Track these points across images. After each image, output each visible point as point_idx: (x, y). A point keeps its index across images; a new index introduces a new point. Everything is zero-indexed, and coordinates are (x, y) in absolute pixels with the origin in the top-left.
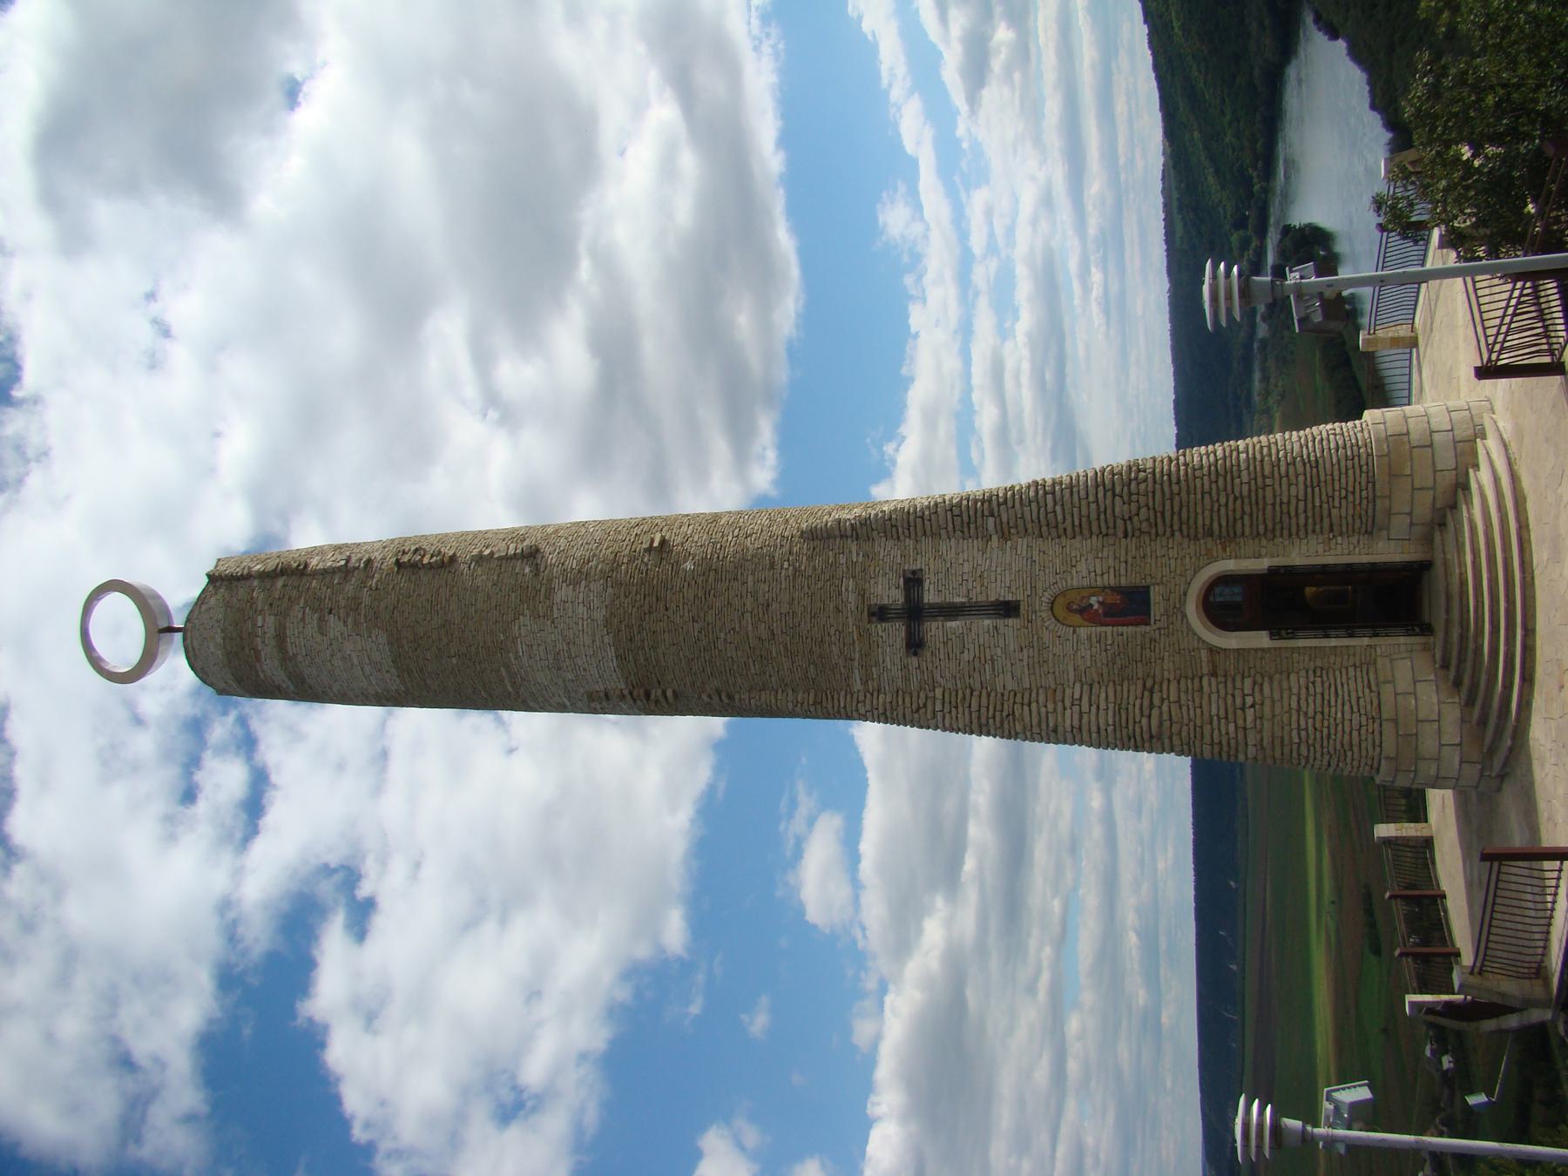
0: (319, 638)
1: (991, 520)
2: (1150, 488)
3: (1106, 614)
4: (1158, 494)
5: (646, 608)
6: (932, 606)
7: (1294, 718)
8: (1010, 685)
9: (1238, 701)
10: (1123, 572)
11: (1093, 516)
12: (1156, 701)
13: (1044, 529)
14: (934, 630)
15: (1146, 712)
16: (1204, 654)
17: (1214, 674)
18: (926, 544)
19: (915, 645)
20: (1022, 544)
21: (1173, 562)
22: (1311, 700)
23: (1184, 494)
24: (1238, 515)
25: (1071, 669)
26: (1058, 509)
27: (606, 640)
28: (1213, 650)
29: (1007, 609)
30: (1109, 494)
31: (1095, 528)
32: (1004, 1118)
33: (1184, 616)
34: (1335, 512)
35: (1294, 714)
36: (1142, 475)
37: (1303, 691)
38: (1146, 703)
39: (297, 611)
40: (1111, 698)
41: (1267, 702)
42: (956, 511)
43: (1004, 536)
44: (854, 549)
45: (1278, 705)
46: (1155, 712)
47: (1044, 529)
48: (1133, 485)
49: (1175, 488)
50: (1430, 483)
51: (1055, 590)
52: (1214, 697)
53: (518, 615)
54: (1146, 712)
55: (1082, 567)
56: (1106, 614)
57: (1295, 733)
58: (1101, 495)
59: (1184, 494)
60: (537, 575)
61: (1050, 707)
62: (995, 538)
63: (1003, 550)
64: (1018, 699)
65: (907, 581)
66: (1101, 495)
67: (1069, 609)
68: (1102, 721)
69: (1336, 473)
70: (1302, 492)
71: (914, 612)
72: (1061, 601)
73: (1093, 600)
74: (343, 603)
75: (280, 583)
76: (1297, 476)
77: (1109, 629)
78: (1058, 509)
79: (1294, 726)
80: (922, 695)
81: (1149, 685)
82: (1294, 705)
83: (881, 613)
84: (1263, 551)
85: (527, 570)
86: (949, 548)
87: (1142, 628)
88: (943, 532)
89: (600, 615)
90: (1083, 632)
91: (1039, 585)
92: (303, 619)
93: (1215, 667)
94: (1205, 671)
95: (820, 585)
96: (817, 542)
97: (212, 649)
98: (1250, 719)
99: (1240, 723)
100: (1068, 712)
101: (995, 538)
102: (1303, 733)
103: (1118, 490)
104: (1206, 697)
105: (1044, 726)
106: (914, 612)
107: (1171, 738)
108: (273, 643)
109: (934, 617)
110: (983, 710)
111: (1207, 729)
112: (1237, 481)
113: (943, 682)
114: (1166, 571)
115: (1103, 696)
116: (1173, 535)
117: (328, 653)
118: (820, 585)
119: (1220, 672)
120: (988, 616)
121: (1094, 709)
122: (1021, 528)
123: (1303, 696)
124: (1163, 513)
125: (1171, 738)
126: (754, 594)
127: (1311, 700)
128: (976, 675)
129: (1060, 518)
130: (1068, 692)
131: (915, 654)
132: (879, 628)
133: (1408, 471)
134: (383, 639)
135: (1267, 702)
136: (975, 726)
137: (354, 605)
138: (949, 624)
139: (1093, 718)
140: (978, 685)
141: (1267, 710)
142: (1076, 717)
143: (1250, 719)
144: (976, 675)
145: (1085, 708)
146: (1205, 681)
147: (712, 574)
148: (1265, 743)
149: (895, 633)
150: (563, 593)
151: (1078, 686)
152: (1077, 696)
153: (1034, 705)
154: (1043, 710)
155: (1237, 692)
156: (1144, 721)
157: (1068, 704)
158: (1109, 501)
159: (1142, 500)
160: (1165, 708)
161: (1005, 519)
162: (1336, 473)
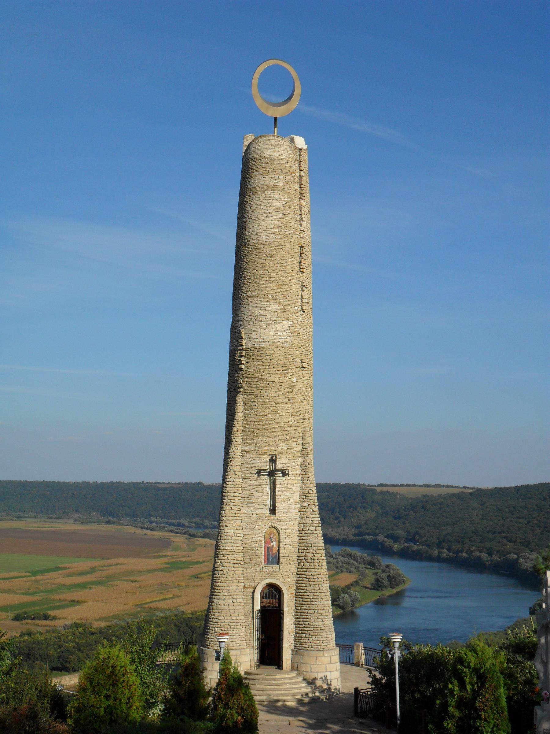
0: (273, 208)
1: (306, 505)
2: (316, 567)
3: (268, 547)
4: (313, 570)
5: (279, 362)
6: (275, 479)
7: (229, 618)
8: (243, 509)
9: (234, 597)
11: (306, 545)
12: (236, 565)
14: (266, 480)
15: (232, 562)
16: (252, 584)
17: (244, 588)
18: (299, 479)
20: (297, 517)
21: (288, 574)
22: (235, 624)
23: (313, 580)
24: (304, 599)
25: (249, 533)
26: (310, 532)
27: (267, 343)
29: (273, 510)
30: (314, 552)
31: (301, 545)
32: (110, 623)
33: (267, 578)
34: (304, 635)
35: (230, 618)
36: (320, 564)
37: (238, 621)
38: (235, 562)
39: (285, 197)
40: (237, 548)
41: (234, 608)
43: (301, 510)
44: (298, 449)
46: (231, 565)
48: (318, 561)
49: (315, 577)
50: (313, 671)
51: (279, 528)
52: (236, 587)
53: (279, 304)
54: (232, 562)
56: (268, 547)
57: (223, 618)
58: (314, 548)
59: (313, 580)
60: (294, 313)
62: (300, 506)
64: (238, 512)
66: (314, 548)
67: (271, 534)
68: (228, 544)
69: (318, 637)
70: (312, 624)
72: (275, 531)
73: (274, 543)
74: (287, 220)
75: (297, 187)
76: (318, 622)
77: (263, 549)
79: (225, 618)
80: (240, 474)
81: (242, 563)
82: (233, 618)
83: (273, 460)
84: (290, 608)
85: (296, 308)
86: (297, 488)
87: (263, 561)
89: (277, 341)
90: (263, 539)
91: (281, 523)
92: (281, 200)
93: (247, 588)
94: (246, 584)
95: (285, 435)
96: (301, 434)
97: (269, 151)
98: (228, 601)
99: (227, 597)
100: (232, 531)
101: (300, 506)
102: (223, 621)
103: (316, 555)
104: (237, 584)
105: (227, 521)
108: (271, 183)
110: (233, 498)
111: (225, 585)
112: (317, 600)
113: (245, 482)
114: (284, 571)
115: (238, 545)
116: (297, 574)
117: (266, 211)
118: (285, 435)
119: (245, 590)
121: (233, 541)
122: (303, 516)
123: (236, 621)
124: (306, 571)
126: (282, 408)
127: (235, 624)
129: (306, 532)
130: (240, 532)
133: (318, 663)
134: (271, 239)
135: (234, 608)
137: (286, 227)
138: (268, 487)
139: (229, 541)
140: (243, 496)
141: (231, 607)
143: (228, 601)
144: (247, 496)
145: (233, 538)
146: (243, 584)
147: (291, 390)
148: (219, 606)
149: (266, 465)
150: (287, 325)
153: (235, 518)
156: (228, 561)
157: (236, 531)
158: (311, 551)
159: (312, 564)
160: (233, 569)
161: (307, 510)
162: (318, 637)
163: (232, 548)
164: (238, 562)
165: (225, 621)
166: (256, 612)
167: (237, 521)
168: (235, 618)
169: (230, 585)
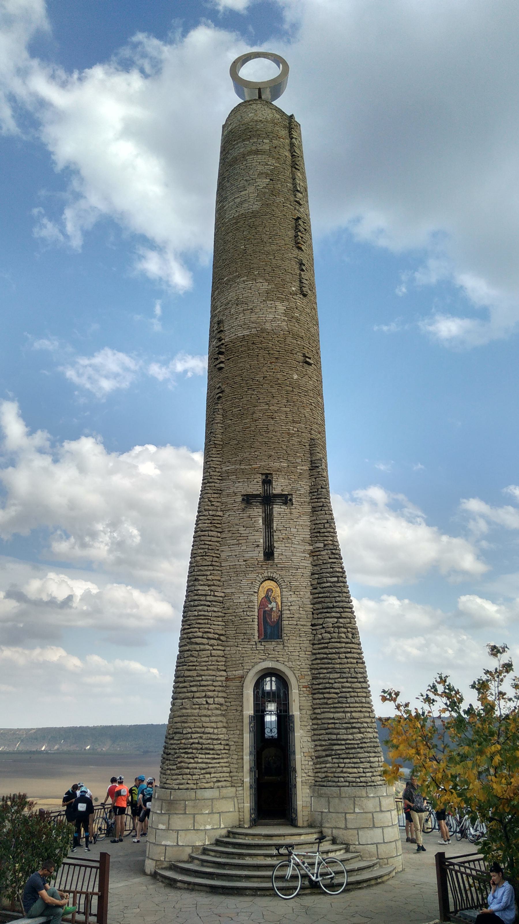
6: (271, 510)
10: (290, 623)
13: (317, 576)
14: (257, 512)
18: (308, 509)
19: (248, 500)
25: (233, 590)
28: (242, 678)
38: (211, 636)
41: (209, 713)
42: (326, 525)
45: (207, 719)
46: (205, 641)
47: (317, 576)
54: (205, 635)
55: (294, 598)
57: (190, 730)
61: (209, 577)
62: (311, 548)
63: (304, 552)
64: (215, 559)
65: (286, 496)
68: (200, 608)
71: (268, 500)
78: (329, 584)
81: (222, 638)
83: (267, 481)
86: (305, 521)
88: (314, 518)
94: (230, 673)
99: (197, 695)
100: (207, 588)
104: (214, 673)
106: (268, 500)
107: (188, 651)
109: (264, 511)
110: (209, 538)
111: (194, 673)
115: (216, 609)
119: (229, 683)
120: (265, 542)
125: (188, 651)
128: (230, 535)
131: (243, 500)
132: (259, 478)
135: (209, 713)
136: (200, 533)
138: (261, 521)
141: (204, 712)
142: (203, 593)
144: (230, 535)
145: (208, 598)
146: (224, 673)
151: (223, 595)
152: (216, 594)
153: (211, 568)
154: (208, 573)
155: (216, 693)
156: (200, 634)
160: (207, 647)
163: (206, 613)
164: (217, 636)
165: (194, 736)
166: (246, 721)
167: (215, 572)
168: (211, 730)
169: (202, 673)
